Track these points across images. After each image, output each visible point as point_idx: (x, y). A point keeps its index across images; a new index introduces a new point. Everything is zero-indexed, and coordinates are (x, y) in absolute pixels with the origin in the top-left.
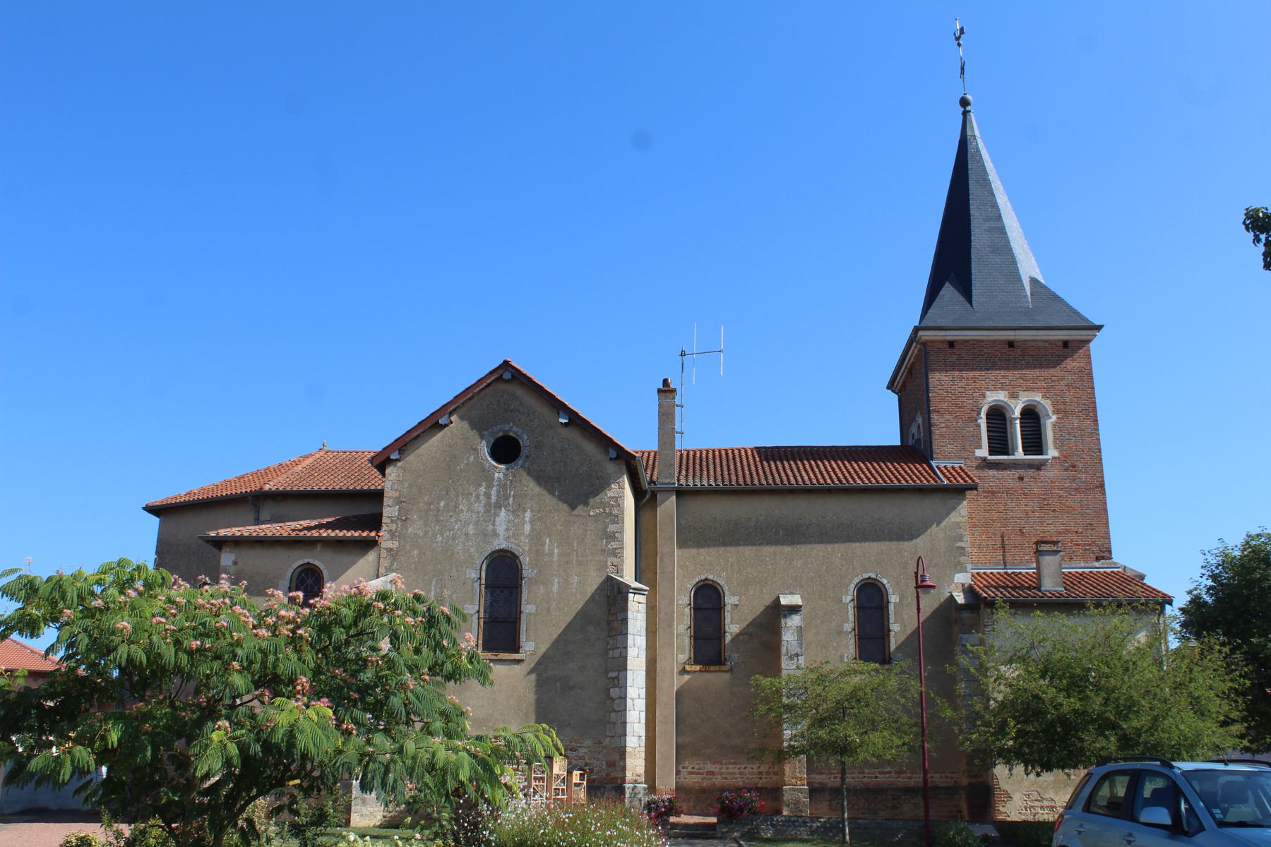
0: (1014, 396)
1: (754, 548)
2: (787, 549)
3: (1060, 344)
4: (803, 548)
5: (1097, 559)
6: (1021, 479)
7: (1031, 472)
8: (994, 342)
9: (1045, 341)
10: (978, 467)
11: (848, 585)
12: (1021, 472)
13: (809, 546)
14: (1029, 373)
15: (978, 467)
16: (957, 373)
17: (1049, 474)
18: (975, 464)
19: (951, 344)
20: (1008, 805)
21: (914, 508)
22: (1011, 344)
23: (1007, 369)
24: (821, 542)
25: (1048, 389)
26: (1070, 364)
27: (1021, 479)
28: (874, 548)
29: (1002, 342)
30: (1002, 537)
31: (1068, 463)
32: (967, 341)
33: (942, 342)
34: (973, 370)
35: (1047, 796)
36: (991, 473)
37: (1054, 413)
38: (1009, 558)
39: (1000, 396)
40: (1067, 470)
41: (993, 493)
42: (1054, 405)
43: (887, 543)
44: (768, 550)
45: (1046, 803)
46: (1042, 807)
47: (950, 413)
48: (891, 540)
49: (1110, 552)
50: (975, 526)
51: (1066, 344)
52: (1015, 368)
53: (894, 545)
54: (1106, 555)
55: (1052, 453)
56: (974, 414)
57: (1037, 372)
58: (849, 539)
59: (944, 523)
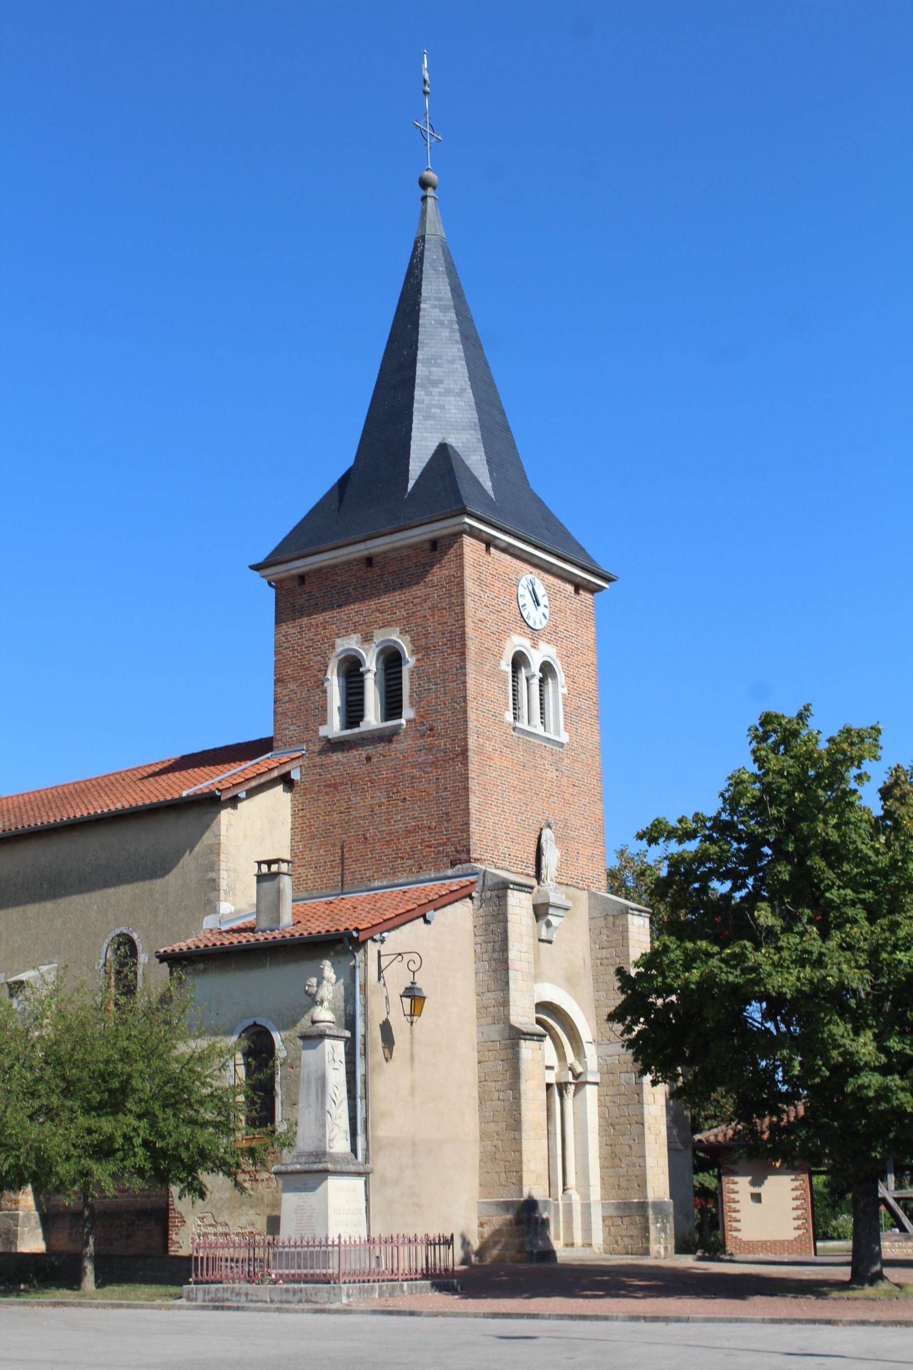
0: (367, 639)
1: (20, 909)
2: (49, 905)
3: (427, 546)
4: (64, 902)
5: (453, 864)
6: (369, 759)
7: (381, 748)
8: (349, 563)
9: (410, 547)
10: (322, 752)
11: (101, 946)
12: (370, 750)
13: (68, 899)
14: (386, 600)
15: (322, 752)
16: (305, 620)
17: (401, 745)
18: (317, 748)
19: (302, 578)
20: (181, 1232)
21: (169, 830)
22: (369, 561)
23: (362, 599)
24: (80, 892)
25: (407, 618)
26: (438, 574)
27: (369, 759)
28: (124, 893)
29: (358, 560)
30: (342, 848)
31: (425, 728)
32: (320, 570)
33: (292, 578)
34: (324, 610)
35: (221, 1219)
36: (337, 756)
37: (413, 653)
38: (348, 878)
39: (351, 643)
40: (422, 736)
41: (335, 786)
42: (413, 641)
43: (140, 884)
44: (33, 909)
45: (220, 1229)
46: (215, 1234)
47: (294, 679)
48: (143, 878)
49: (468, 851)
50: (313, 837)
51: (434, 544)
52: (371, 596)
53: (146, 885)
54: (463, 856)
55: (408, 713)
56: (320, 675)
57: (397, 596)
58: (106, 885)
59: (197, 849)
